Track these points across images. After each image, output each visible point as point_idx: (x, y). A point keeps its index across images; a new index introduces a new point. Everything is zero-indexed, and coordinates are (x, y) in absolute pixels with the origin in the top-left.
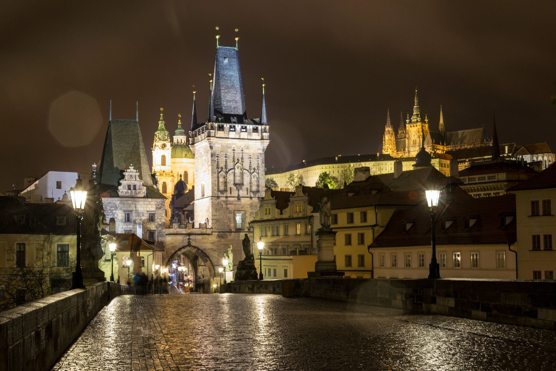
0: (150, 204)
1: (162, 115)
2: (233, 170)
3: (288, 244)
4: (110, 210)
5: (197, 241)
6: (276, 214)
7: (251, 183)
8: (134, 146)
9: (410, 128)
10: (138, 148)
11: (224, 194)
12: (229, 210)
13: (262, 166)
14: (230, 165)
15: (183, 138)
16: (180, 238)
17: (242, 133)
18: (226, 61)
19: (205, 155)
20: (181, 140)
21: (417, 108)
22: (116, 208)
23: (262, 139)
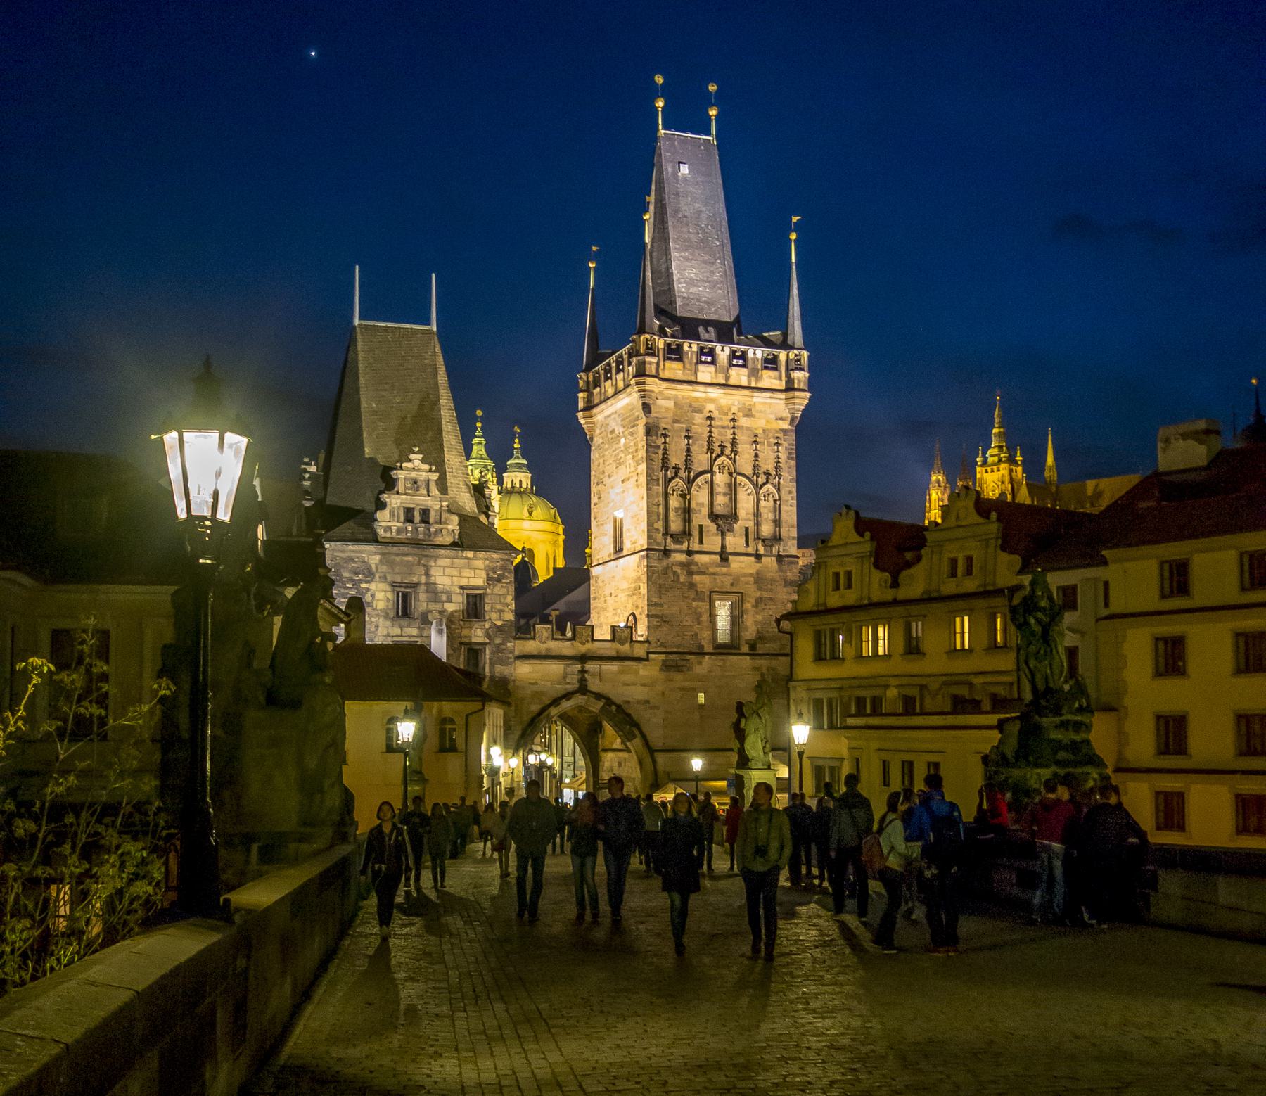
0: (469, 567)
1: (479, 424)
2: (709, 475)
3: (923, 681)
4: (352, 580)
5: (606, 677)
6: (875, 584)
7: (757, 514)
8: (423, 400)
9: (985, 475)
10: (436, 402)
11: (682, 543)
12: (696, 591)
13: (789, 467)
14: (701, 460)
15: (525, 477)
16: (556, 668)
17: (734, 372)
18: (685, 170)
19: (626, 433)
20: (521, 481)
21: (1000, 432)
22: (370, 575)
23: (790, 388)
